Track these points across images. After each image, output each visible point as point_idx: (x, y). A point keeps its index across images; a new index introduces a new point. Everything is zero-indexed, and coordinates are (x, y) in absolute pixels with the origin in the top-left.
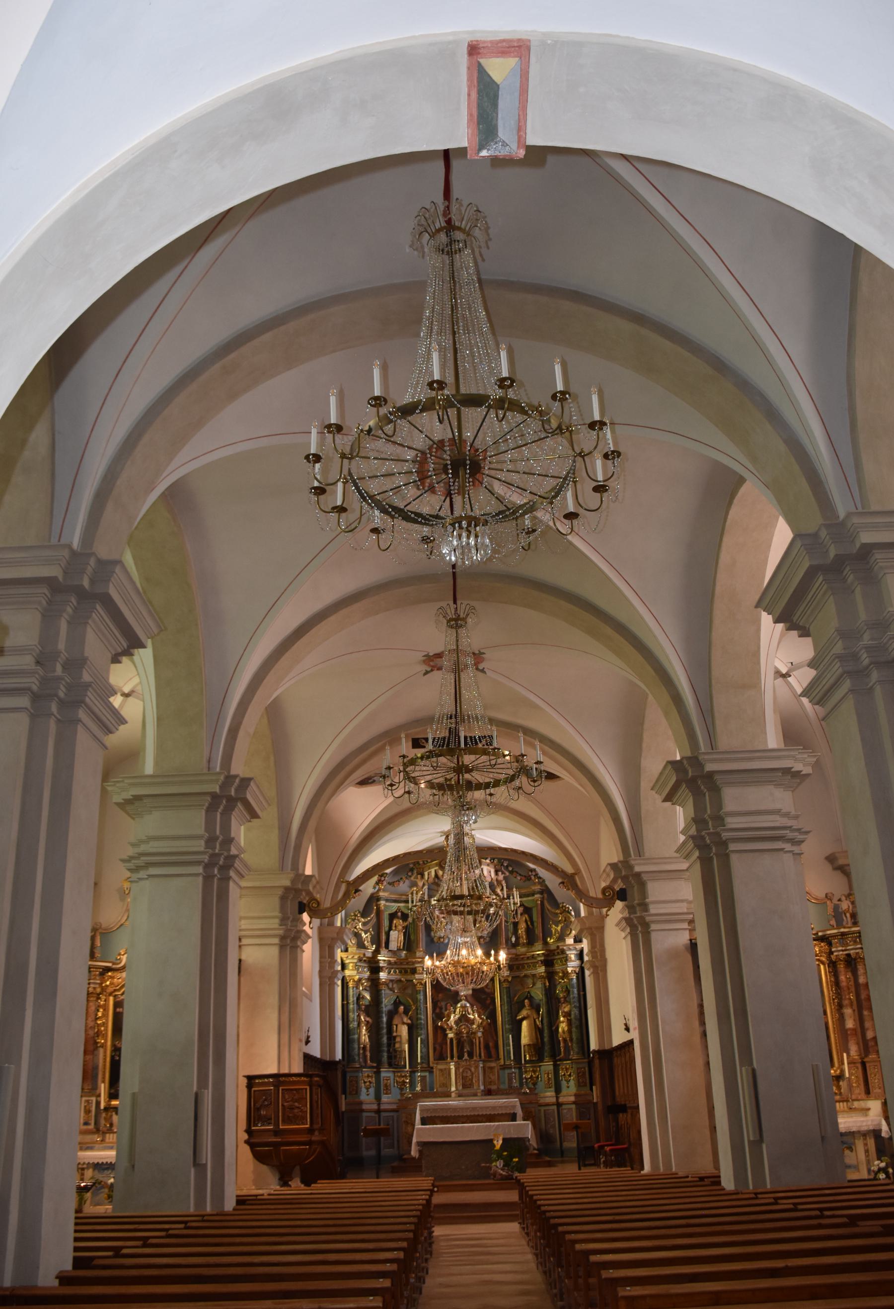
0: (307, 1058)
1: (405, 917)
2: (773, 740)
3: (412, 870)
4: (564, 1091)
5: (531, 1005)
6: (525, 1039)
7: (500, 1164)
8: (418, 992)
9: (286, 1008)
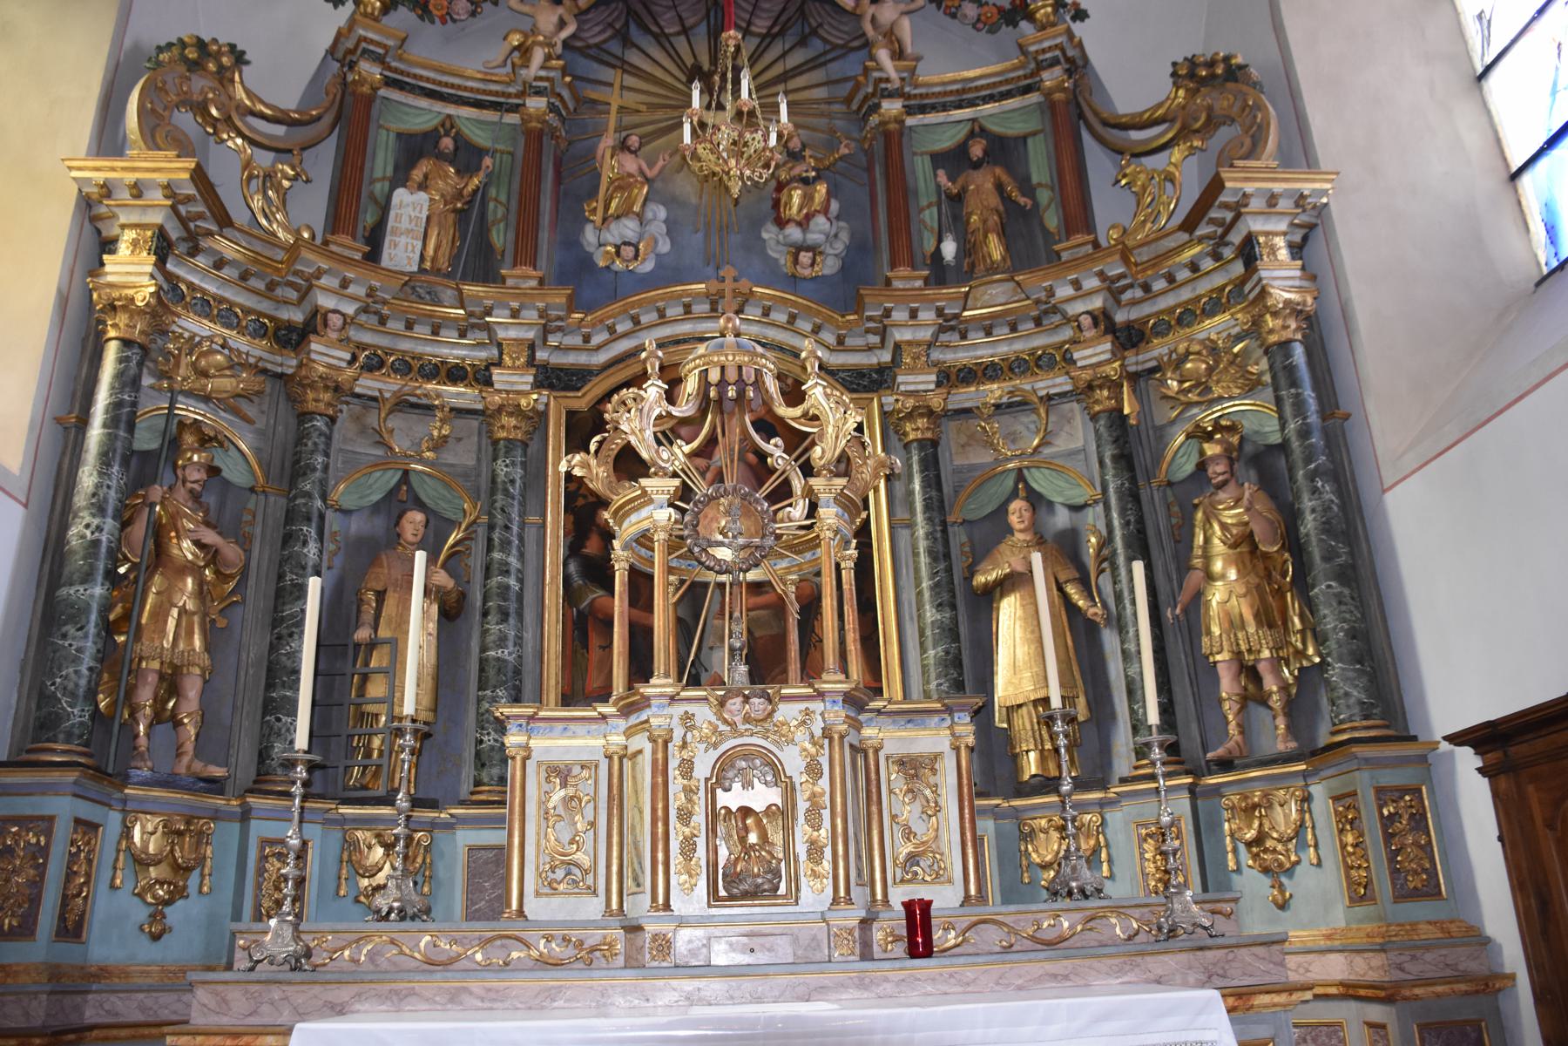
1: (467, 156)
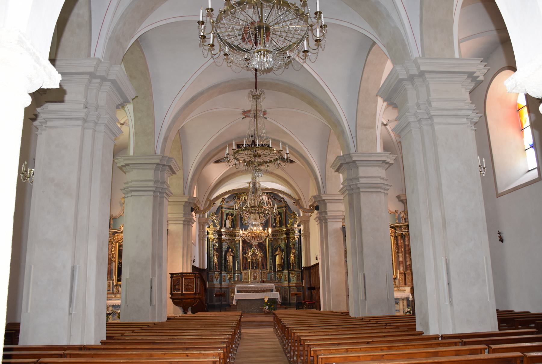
0: (194, 268)
1: (232, 215)
2: (379, 149)
3: (235, 197)
4: (292, 282)
5: (280, 250)
6: (277, 262)
7: (267, 307)
8: (237, 244)
9: (186, 249)
